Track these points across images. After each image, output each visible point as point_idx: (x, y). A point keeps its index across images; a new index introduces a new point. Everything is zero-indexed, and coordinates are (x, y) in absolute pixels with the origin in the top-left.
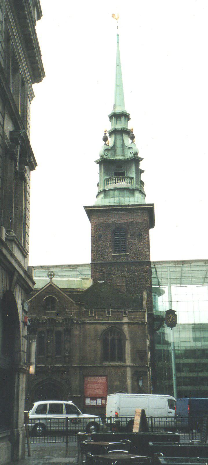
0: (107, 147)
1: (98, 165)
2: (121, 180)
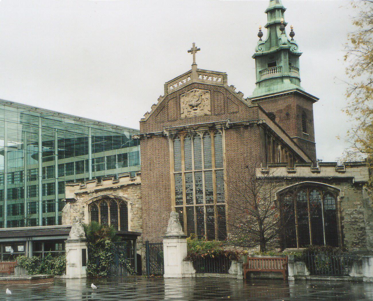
0: (261, 42)
1: (254, 59)
2: (273, 70)
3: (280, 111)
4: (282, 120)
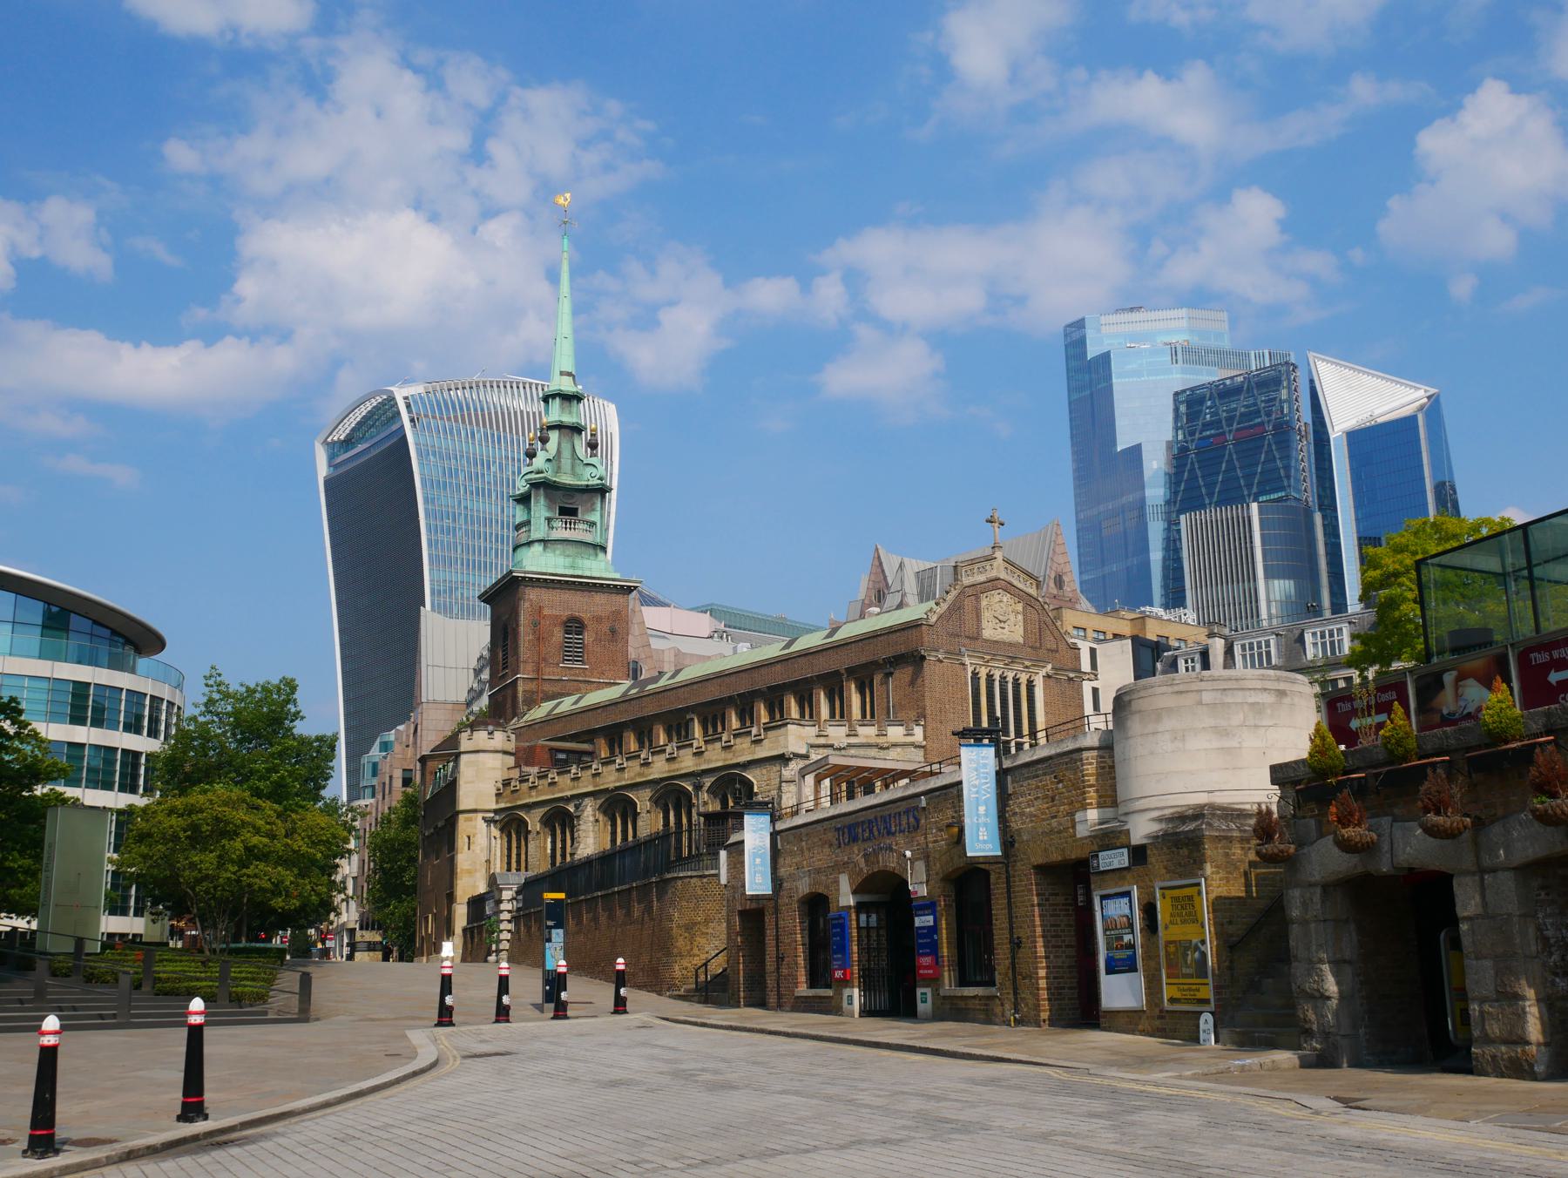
3: (598, 619)
4: (601, 641)
